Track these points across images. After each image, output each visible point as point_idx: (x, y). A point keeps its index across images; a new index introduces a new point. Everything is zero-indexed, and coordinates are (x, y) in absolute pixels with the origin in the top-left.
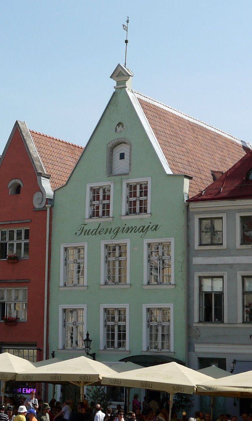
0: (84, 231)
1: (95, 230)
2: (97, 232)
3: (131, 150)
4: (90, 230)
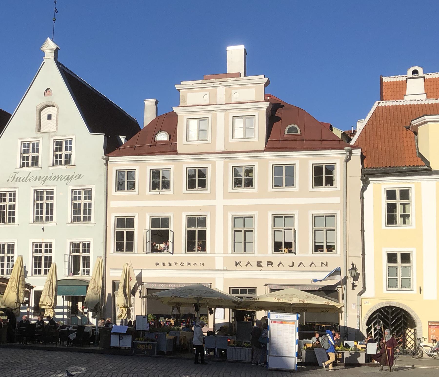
0: (16, 178)
1: (26, 178)
2: (26, 179)
3: (58, 112)
4: (21, 178)
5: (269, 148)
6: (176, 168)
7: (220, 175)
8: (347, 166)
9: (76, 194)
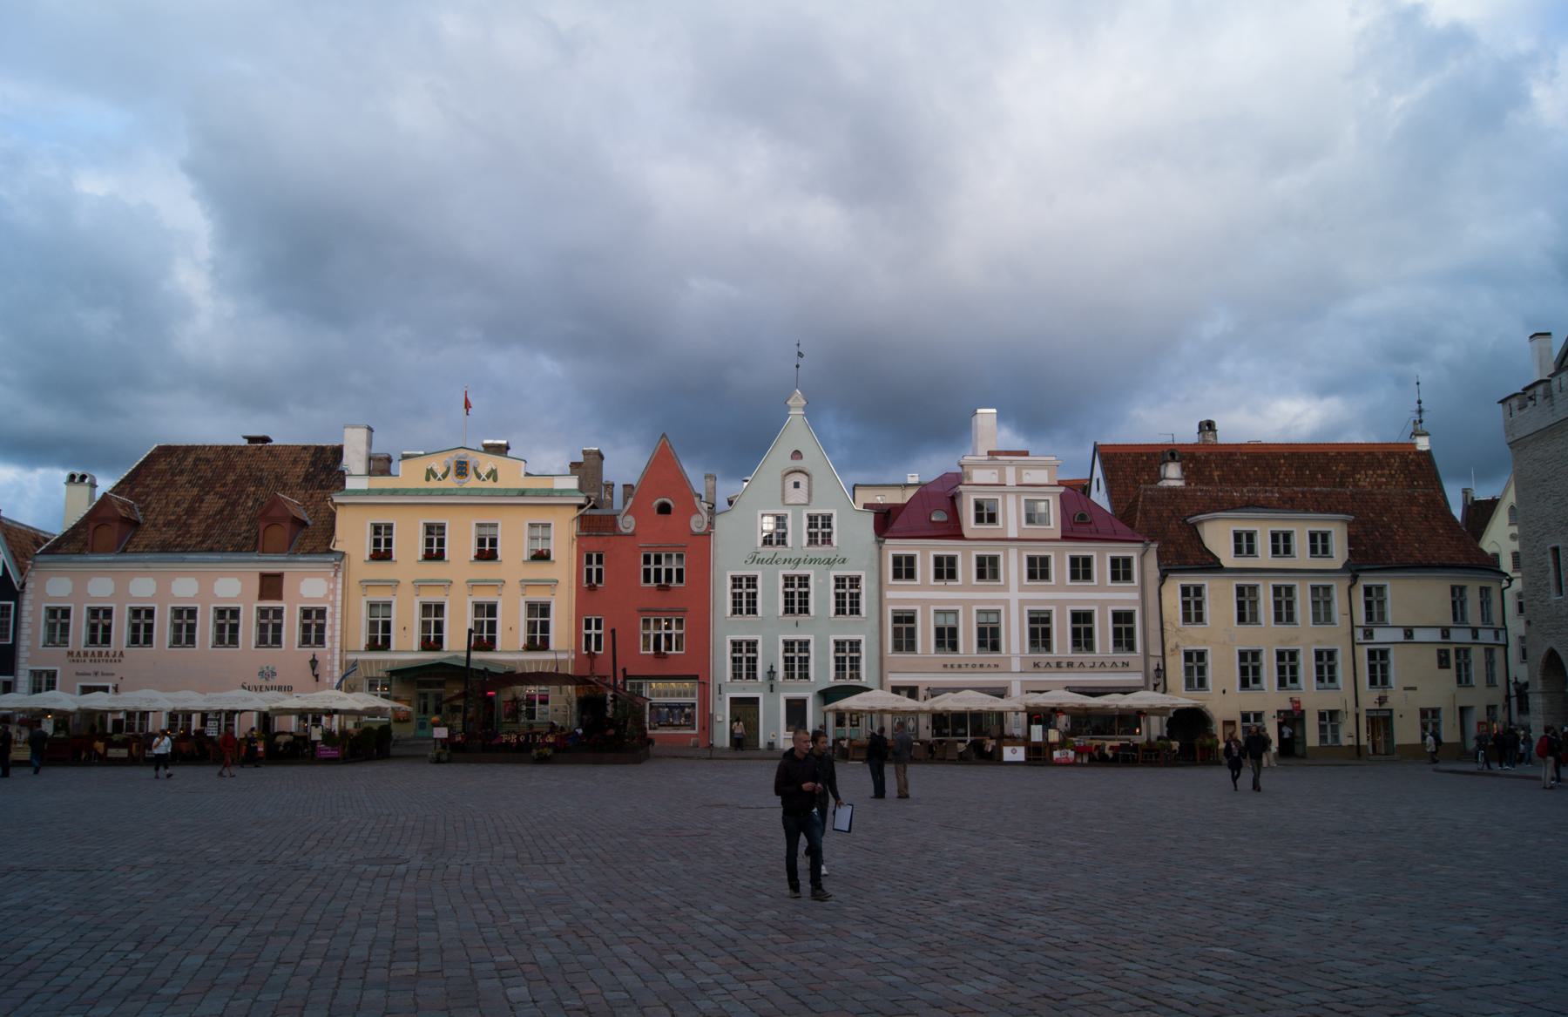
2: (771, 561)
5: (1065, 538)
6: (966, 557)
7: (1013, 566)
8: (1144, 558)
9: (840, 582)
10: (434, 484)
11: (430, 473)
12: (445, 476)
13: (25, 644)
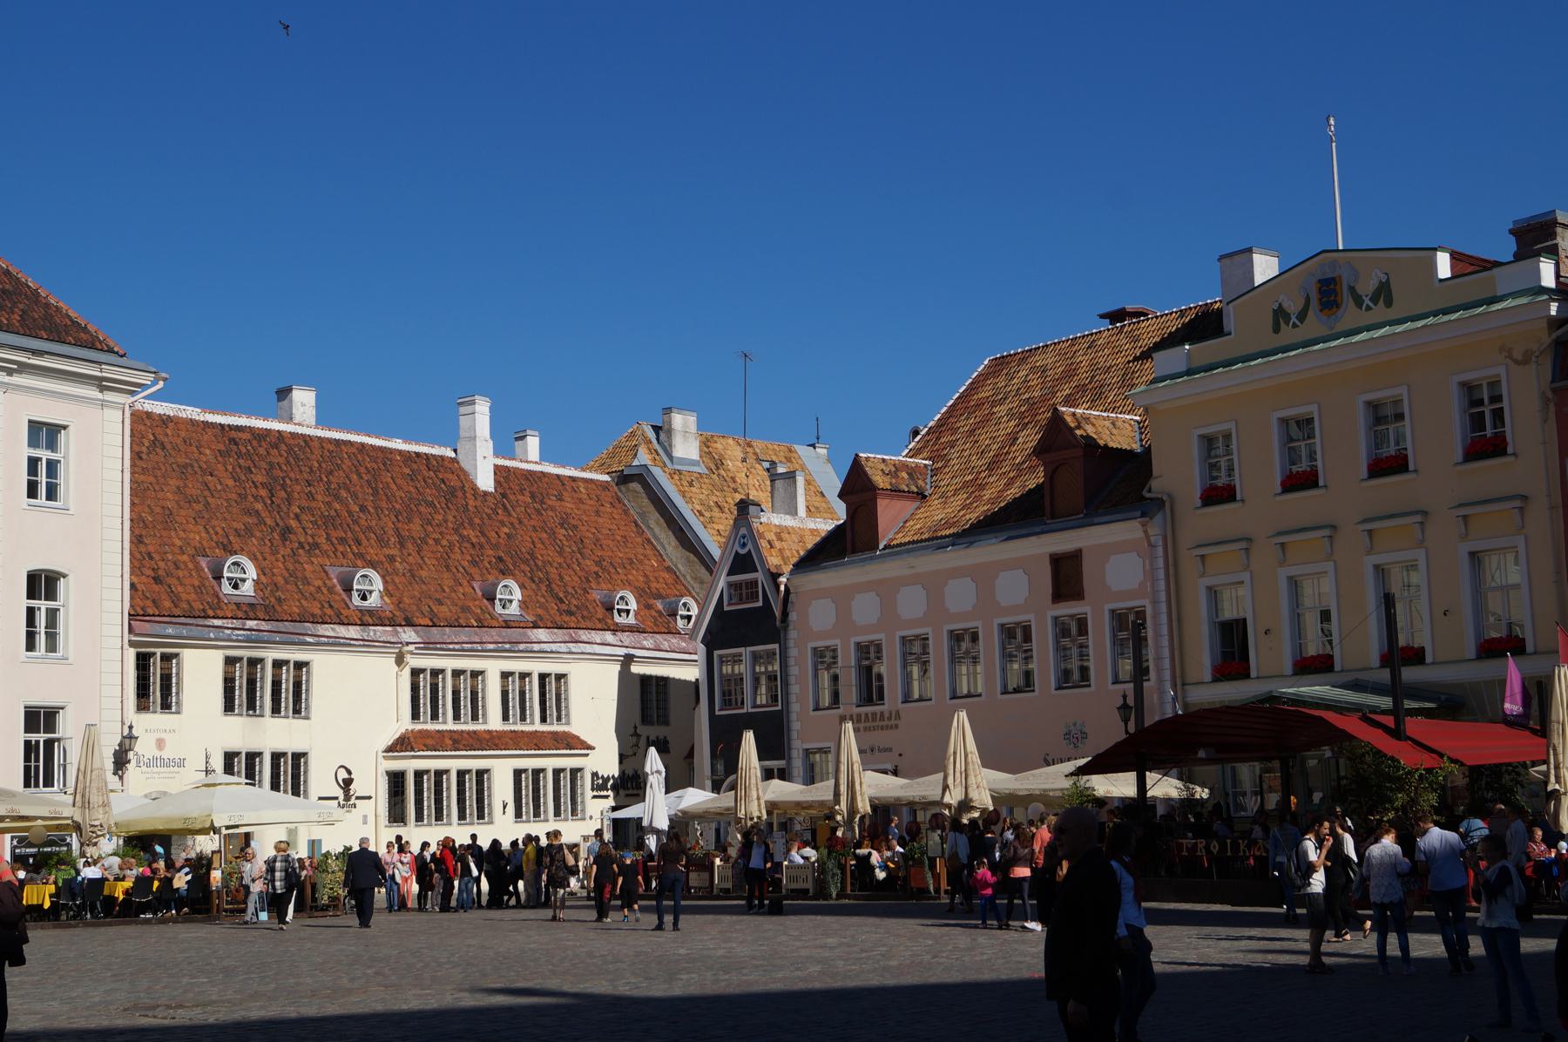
10: (1288, 334)
11: (1280, 315)
12: (1302, 316)
13: (795, 707)
